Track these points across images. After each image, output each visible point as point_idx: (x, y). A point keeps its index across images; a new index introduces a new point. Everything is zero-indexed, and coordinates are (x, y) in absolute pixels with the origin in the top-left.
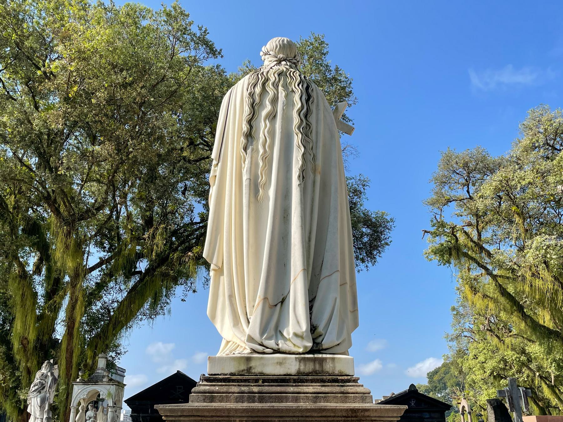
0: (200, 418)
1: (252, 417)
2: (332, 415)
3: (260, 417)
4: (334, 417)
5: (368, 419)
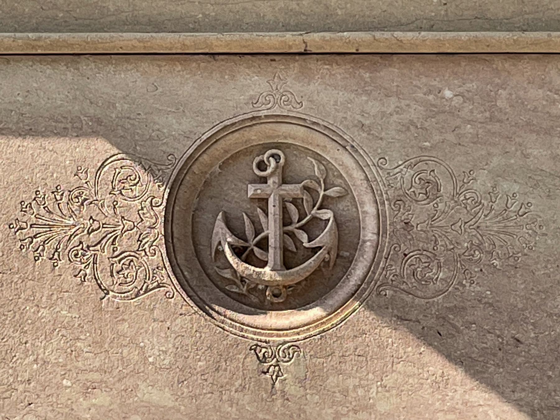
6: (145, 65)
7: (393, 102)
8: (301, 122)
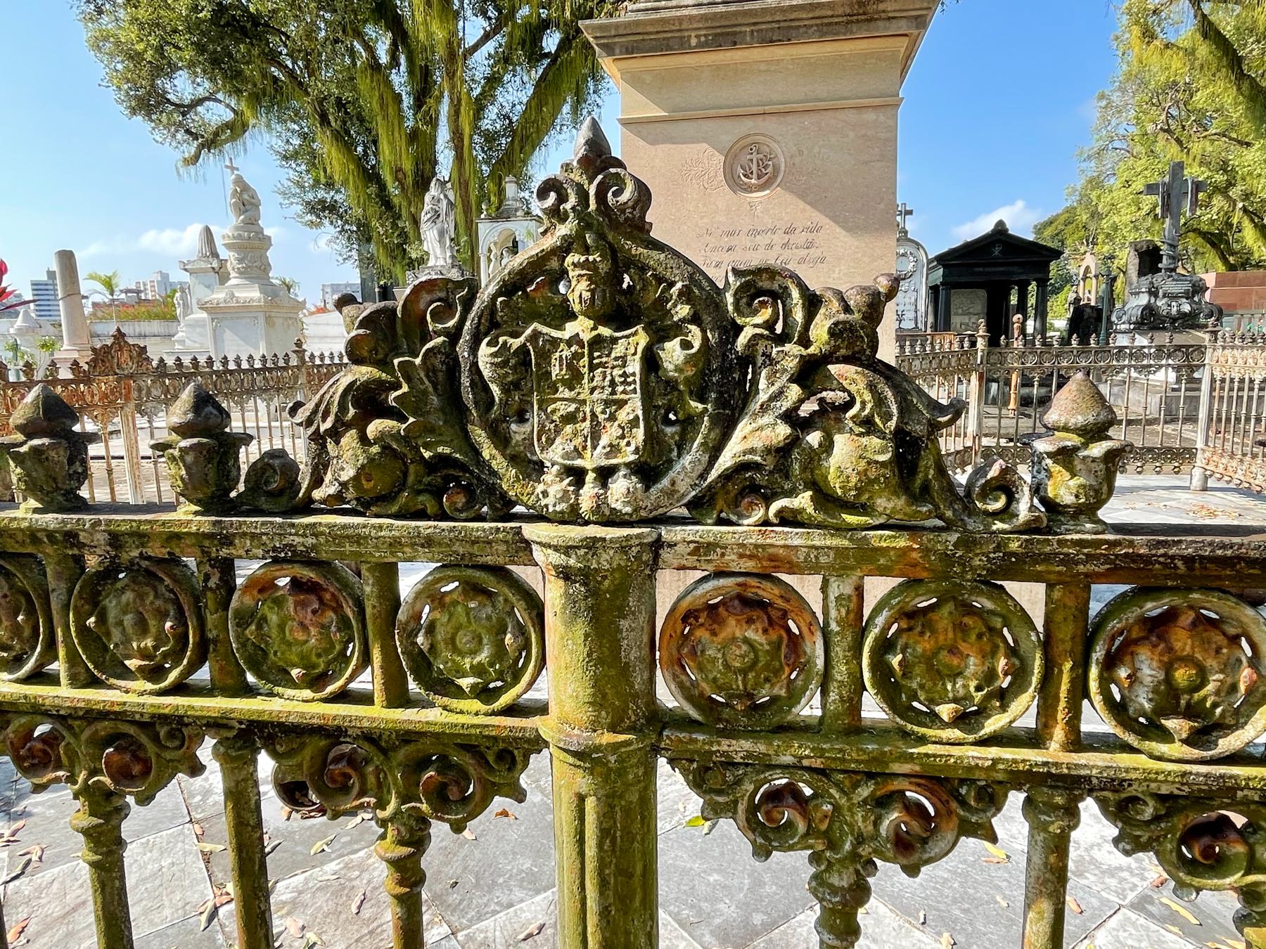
0: (641, 37)
1: (713, 28)
2: (830, 13)
3: (724, 26)
4: (832, 16)
5: (883, 15)
6: (717, 120)
7: (790, 127)
8: (763, 135)
